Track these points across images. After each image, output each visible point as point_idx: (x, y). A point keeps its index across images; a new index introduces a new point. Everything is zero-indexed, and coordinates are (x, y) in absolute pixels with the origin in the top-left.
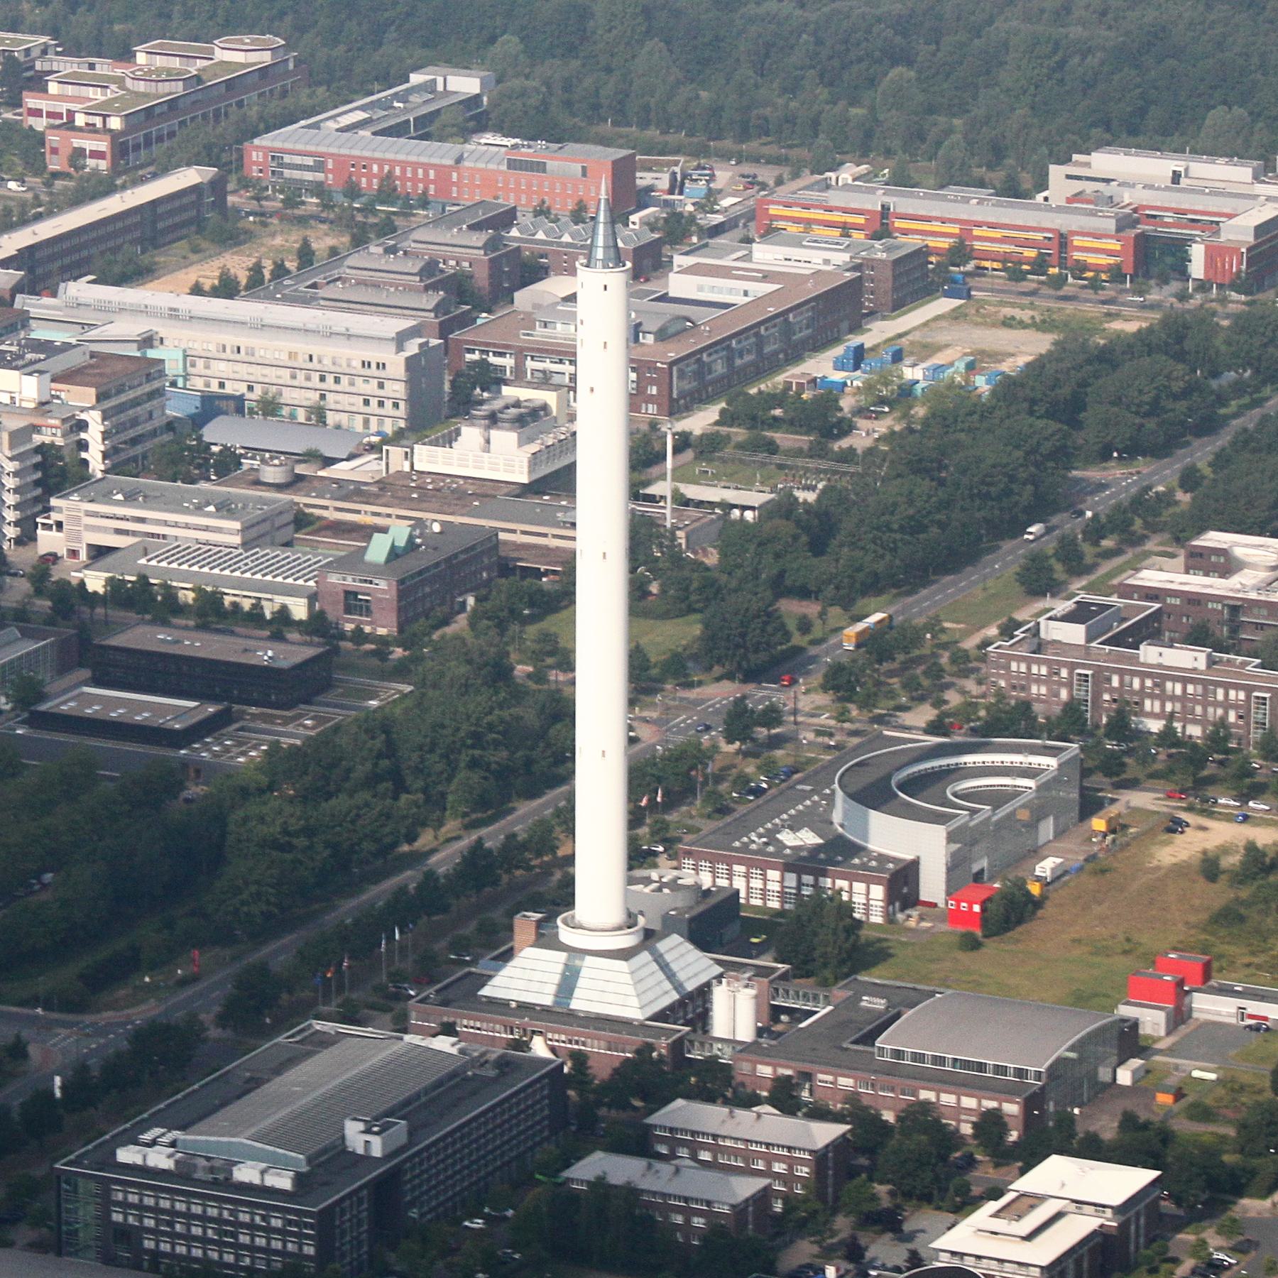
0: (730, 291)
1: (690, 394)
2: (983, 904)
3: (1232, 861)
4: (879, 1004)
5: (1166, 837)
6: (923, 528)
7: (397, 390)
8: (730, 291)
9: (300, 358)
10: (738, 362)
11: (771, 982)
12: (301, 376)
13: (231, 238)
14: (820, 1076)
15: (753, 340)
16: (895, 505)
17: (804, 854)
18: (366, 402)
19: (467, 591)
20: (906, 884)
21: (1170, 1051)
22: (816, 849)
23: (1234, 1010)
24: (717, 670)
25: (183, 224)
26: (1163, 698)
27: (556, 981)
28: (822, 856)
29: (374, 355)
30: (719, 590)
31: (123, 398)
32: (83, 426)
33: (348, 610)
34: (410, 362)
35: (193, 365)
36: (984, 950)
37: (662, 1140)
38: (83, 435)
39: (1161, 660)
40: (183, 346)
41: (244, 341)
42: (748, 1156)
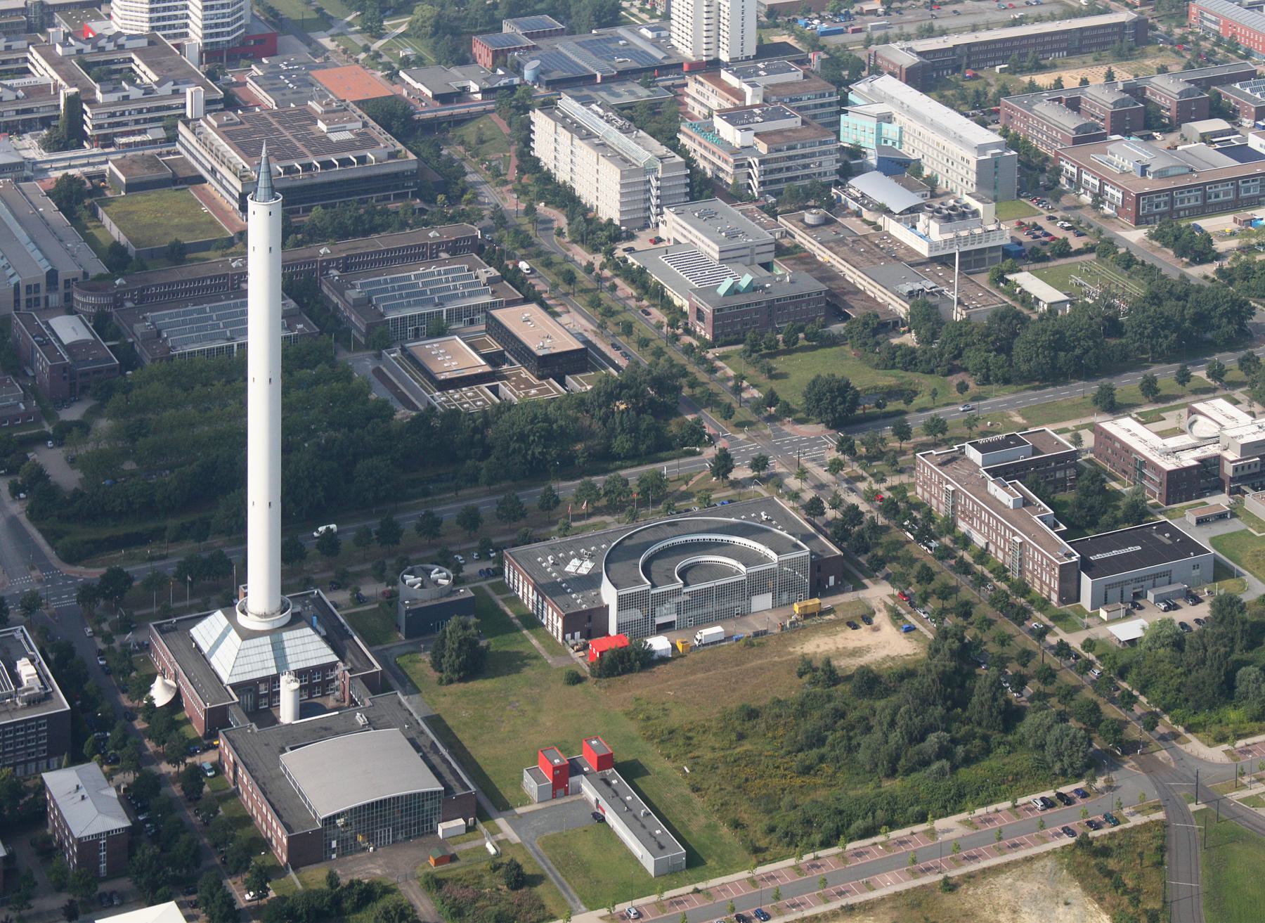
2: (601, 653)
20: (590, 620)
25: (1091, 46)
31: (791, 153)
34: (979, 162)
36: (578, 687)
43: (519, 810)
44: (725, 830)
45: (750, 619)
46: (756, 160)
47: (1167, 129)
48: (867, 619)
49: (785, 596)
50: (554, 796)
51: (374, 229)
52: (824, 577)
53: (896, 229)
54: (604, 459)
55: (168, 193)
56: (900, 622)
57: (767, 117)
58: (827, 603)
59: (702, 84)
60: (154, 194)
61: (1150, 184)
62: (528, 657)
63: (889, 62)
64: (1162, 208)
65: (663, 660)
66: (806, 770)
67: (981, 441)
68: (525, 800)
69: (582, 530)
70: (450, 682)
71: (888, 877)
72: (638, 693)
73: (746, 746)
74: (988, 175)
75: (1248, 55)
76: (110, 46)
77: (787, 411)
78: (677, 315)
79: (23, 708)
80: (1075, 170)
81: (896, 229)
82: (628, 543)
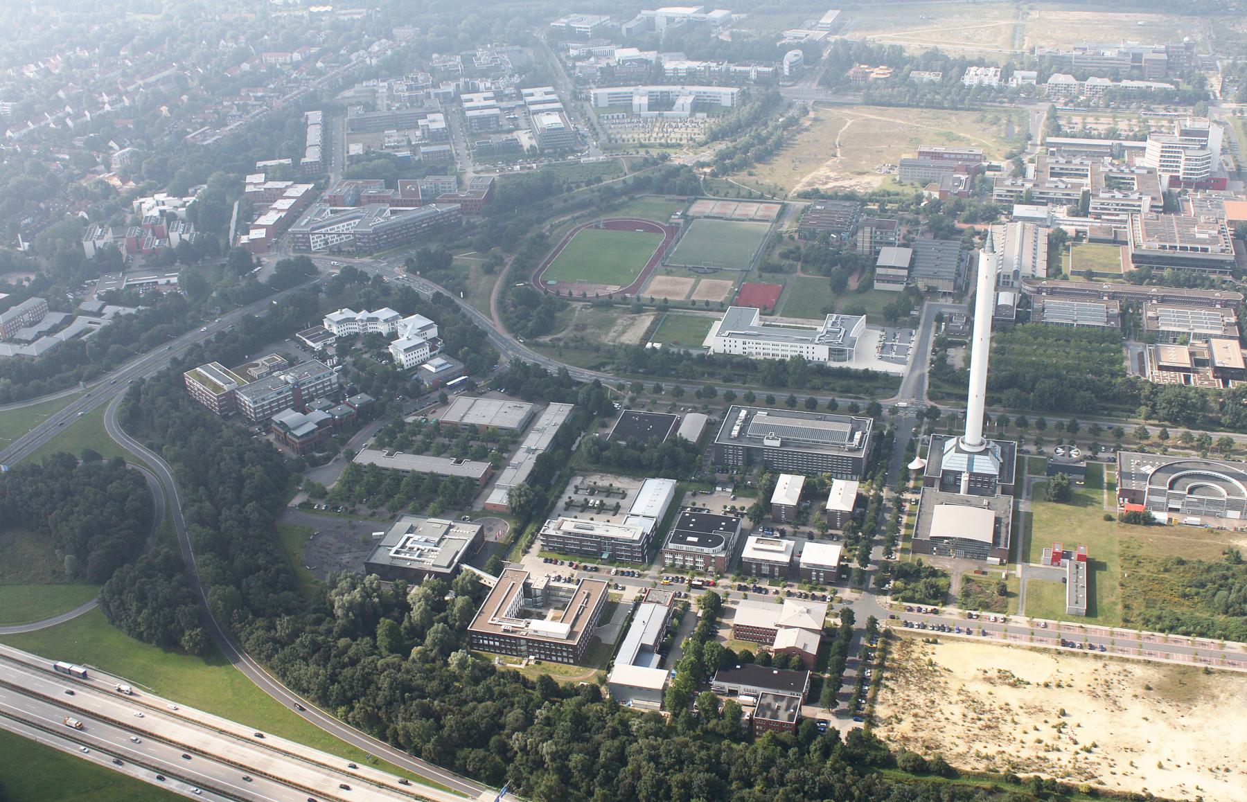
44: (1120, 607)
45: (1223, 521)
51: (1195, 286)
54: (1214, 425)
55: (1109, 246)
60: (1102, 246)
65: (1160, 524)
66: (1185, 596)
69: (1175, 454)
71: (1181, 656)
72: (1133, 534)
73: (1167, 575)
76: (1127, 171)
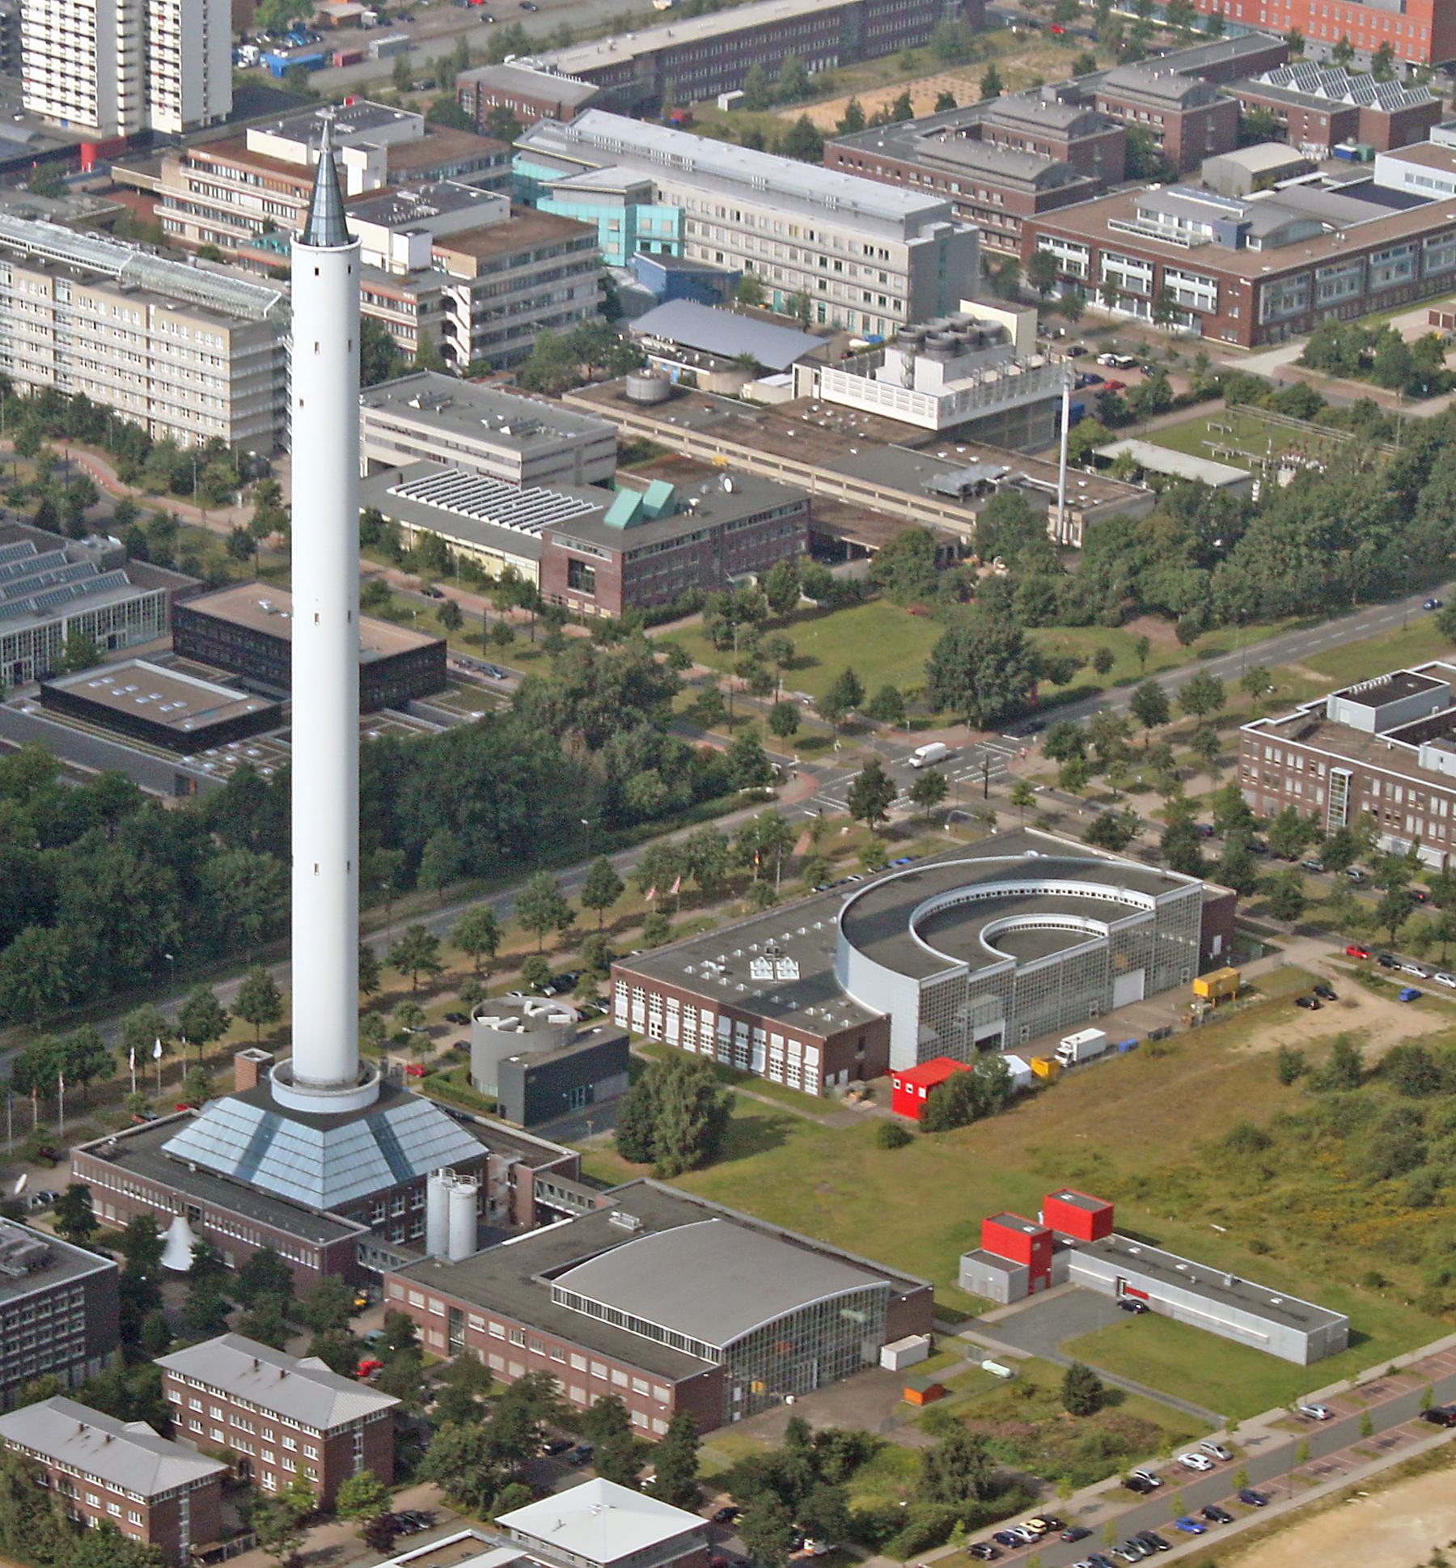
0: (1441, 185)
1: (1293, 320)
3: (1323, 1061)
4: (629, 1222)
5: (1295, 1009)
6: (1350, 543)
7: (899, 286)
8: (1441, 185)
9: (801, 234)
10: (1378, 282)
11: (535, 1174)
12: (801, 255)
13: (955, 56)
14: (472, 1317)
15: (1409, 254)
16: (1308, 511)
17: (758, 993)
18: (867, 297)
19: (748, 570)
21: (996, 1329)
22: (788, 988)
23: (1112, 1280)
24: (948, 715)
25: (897, 36)
26: (1427, 817)
27: (278, 1136)
28: (776, 999)
29: (878, 240)
30: (1052, 599)
31: (521, 271)
32: (449, 304)
33: (573, 583)
34: (914, 252)
35: (692, 229)
36: (908, 1150)
37: (177, 1386)
38: (450, 316)
39: (1441, 767)
40: (683, 204)
41: (745, 206)
42: (260, 1423)
43: (988, 1318)
45: (1117, 1017)
46: (465, 291)
47: (1168, 174)
48: (1324, 991)
49: (1162, 974)
50: (1031, 1292)
52: (1225, 936)
53: (838, 387)
56: (1384, 988)
57: (450, 201)
58: (1251, 971)
59: (207, 167)
61: (1260, 261)
62: (772, 1124)
63: (522, 99)
64: (1297, 307)
65: (1026, 1093)
66: (1425, 1201)
67: (1356, 689)
68: (987, 1305)
70: (678, 1171)
73: (1284, 1187)
74: (936, 278)
75: (1217, 24)
77: (891, 706)
78: (511, 588)
79: (23, 1277)
80: (1082, 257)
81: (838, 387)
82: (857, 914)
